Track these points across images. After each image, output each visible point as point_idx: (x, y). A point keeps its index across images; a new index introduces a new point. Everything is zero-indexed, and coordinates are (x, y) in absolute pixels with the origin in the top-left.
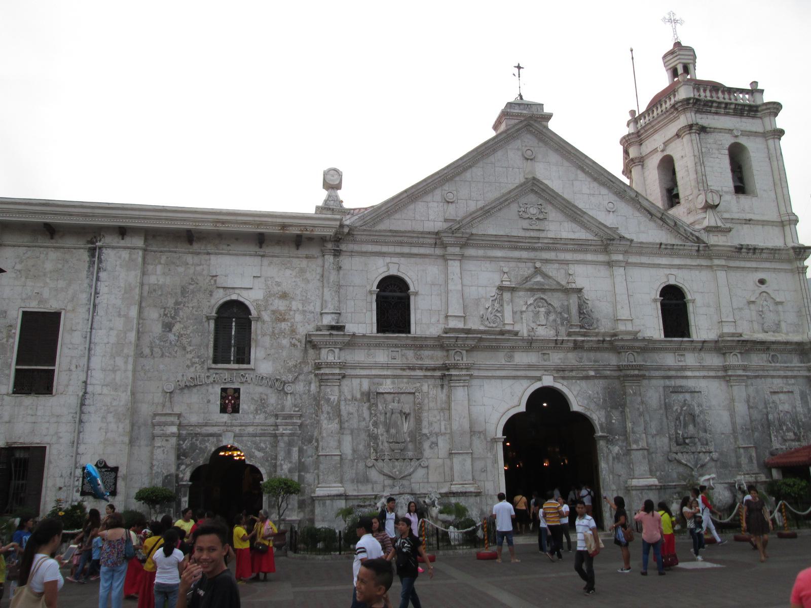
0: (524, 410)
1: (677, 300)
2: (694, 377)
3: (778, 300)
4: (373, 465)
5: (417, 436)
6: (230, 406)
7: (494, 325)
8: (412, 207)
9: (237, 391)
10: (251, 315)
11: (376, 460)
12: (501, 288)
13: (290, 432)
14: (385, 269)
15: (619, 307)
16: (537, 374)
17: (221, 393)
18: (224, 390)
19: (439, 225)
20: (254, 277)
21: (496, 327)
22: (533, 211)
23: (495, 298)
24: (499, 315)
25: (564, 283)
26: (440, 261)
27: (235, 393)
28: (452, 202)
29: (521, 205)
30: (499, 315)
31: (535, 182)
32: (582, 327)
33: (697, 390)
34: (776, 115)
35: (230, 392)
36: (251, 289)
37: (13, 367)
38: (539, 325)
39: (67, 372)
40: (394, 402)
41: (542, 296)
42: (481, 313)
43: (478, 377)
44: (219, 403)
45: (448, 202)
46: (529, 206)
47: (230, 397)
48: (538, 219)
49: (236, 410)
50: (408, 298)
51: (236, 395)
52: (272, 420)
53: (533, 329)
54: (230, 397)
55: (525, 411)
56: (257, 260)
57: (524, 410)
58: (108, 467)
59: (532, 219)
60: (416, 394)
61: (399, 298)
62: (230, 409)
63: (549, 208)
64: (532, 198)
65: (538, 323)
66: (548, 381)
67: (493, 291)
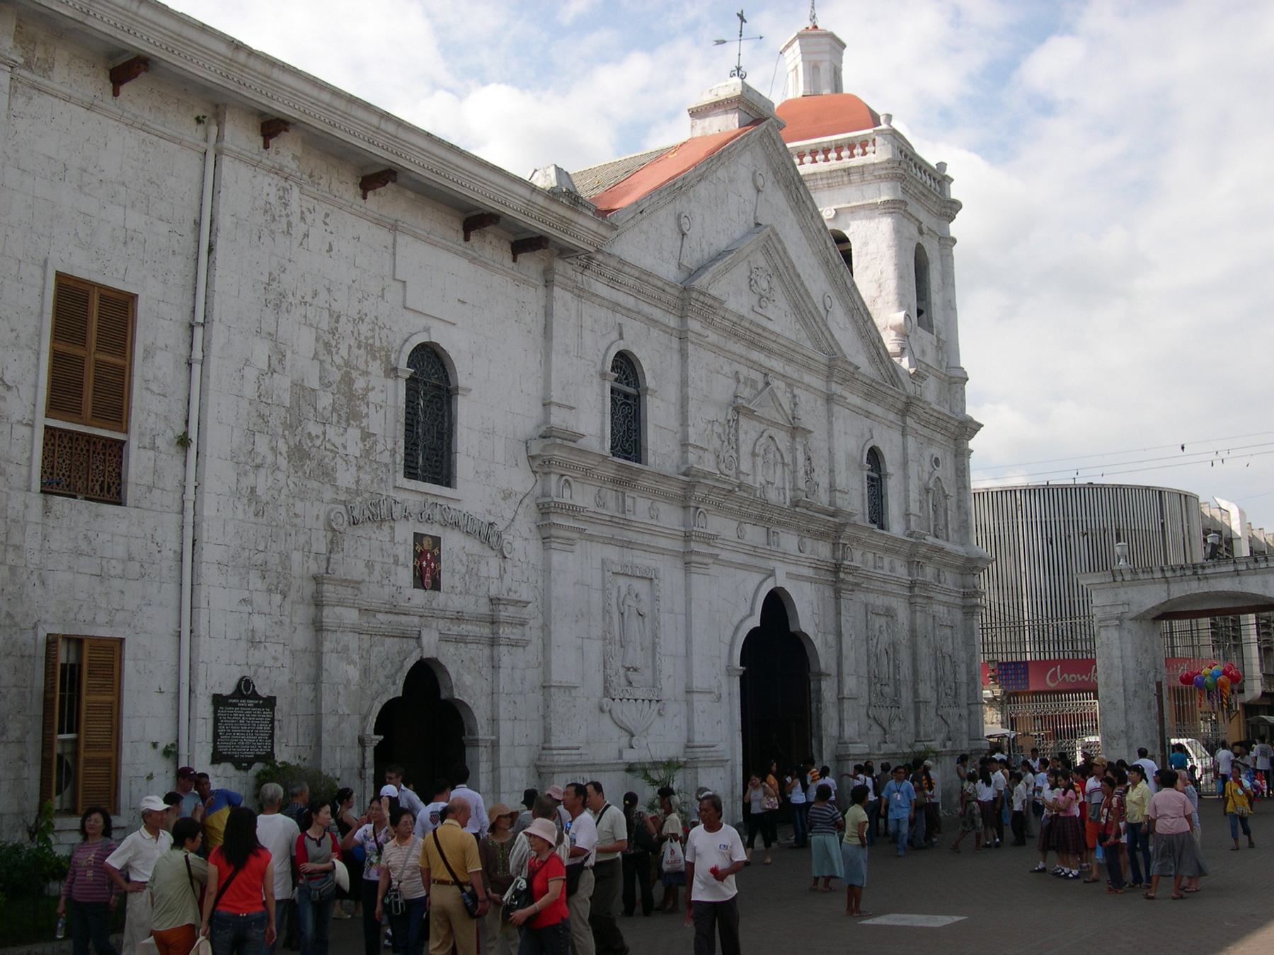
6: (428, 575)
9: (437, 541)
17: (415, 545)
18: (418, 537)
20: (459, 300)
27: (434, 548)
34: (952, 218)
35: (427, 543)
37: (42, 421)
38: (768, 483)
39: (151, 453)
44: (411, 565)
45: (684, 234)
47: (429, 555)
49: (436, 586)
50: (637, 398)
51: (436, 551)
52: (484, 609)
54: (429, 555)
58: (259, 698)
60: (656, 581)
61: (627, 396)
62: (428, 581)
66: (781, 581)
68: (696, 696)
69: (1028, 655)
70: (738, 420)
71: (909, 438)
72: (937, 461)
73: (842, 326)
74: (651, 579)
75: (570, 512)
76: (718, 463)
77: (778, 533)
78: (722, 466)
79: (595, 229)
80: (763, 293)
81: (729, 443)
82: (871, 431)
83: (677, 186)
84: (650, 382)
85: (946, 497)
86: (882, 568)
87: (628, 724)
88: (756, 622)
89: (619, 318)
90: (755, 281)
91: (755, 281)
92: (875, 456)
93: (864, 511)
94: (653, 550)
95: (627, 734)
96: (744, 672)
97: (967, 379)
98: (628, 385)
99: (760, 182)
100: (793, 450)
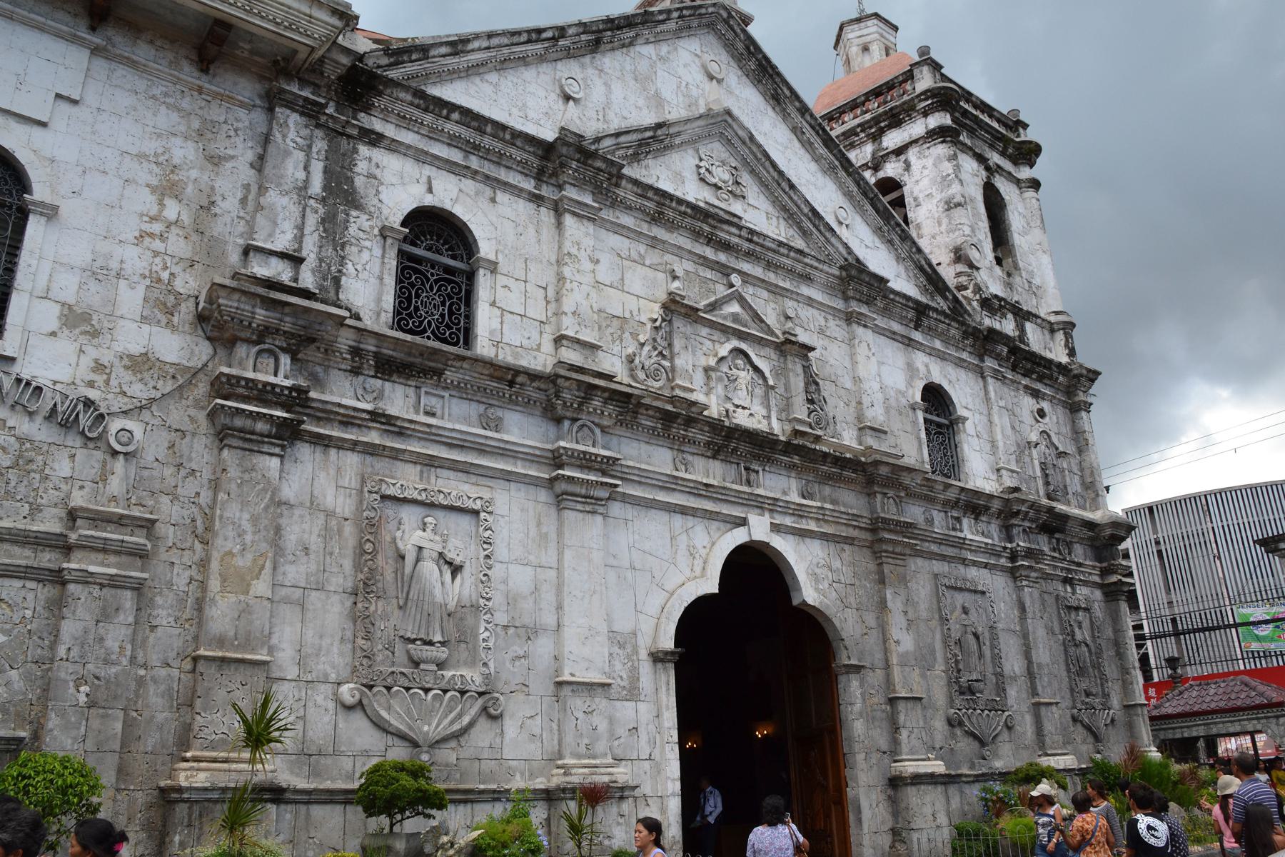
0: (712, 586)
1: (938, 415)
3: (1061, 449)
4: (360, 703)
5: (482, 630)
7: (657, 385)
8: (493, 77)
10: (30, 193)
11: (370, 687)
12: (674, 307)
13: (113, 571)
14: (422, 188)
15: (866, 401)
16: (737, 512)
19: (549, 135)
21: (660, 388)
22: (721, 175)
23: (658, 324)
24: (666, 364)
25: (779, 333)
26: (546, 215)
28: (574, 99)
29: (703, 156)
30: (666, 364)
31: (730, 120)
32: (811, 427)
33: (980, 588)
36: (43, 124)
38: (738, 406)
40: (424, 530)
41: (744, 346)
42: (630, 351)
43: (626, 499)
45: (567, 98)
46: (717, 163)
48: (730, 192)
50: (471, 276)
53: (727, 411)
55: (717, 591)
56: (77, 57)
57: (712, 586)
59: (720, 188)
60: (482, 515)
61: (448, 270)
63: (746, 178)
64: (716, 149)
65: (737, 402)
66: (759, 528)
67: (656, 311)
68: (566, 691)
69: (1241, 662)
70: (670, 321)
71: (990, 380)
72: (1041, 413)
73: (870, 245)
74: (476, 513)
75: (270, 397)
76: (632, 370)
77: (757, 472)
78: (641, 375)
79: (307, 11)
80: (720, 184)
81: (655, 349)
82: (927, 366)
83: (544, 35)
84: (486, 249)
85: (1061, 455)
86: (961, 531)
87: (402, 727)
88: (711, 585)
89: (428, 171)
90: (707, 170)
91: (707, 170)
92: (935, 397)
93: (923, 458)
94: (480, 471)
95: (407, 744)
96: (681, 655)
97: (1073, 325)
98: (454, 257)
99: (714, 68)
100: (781, 372)
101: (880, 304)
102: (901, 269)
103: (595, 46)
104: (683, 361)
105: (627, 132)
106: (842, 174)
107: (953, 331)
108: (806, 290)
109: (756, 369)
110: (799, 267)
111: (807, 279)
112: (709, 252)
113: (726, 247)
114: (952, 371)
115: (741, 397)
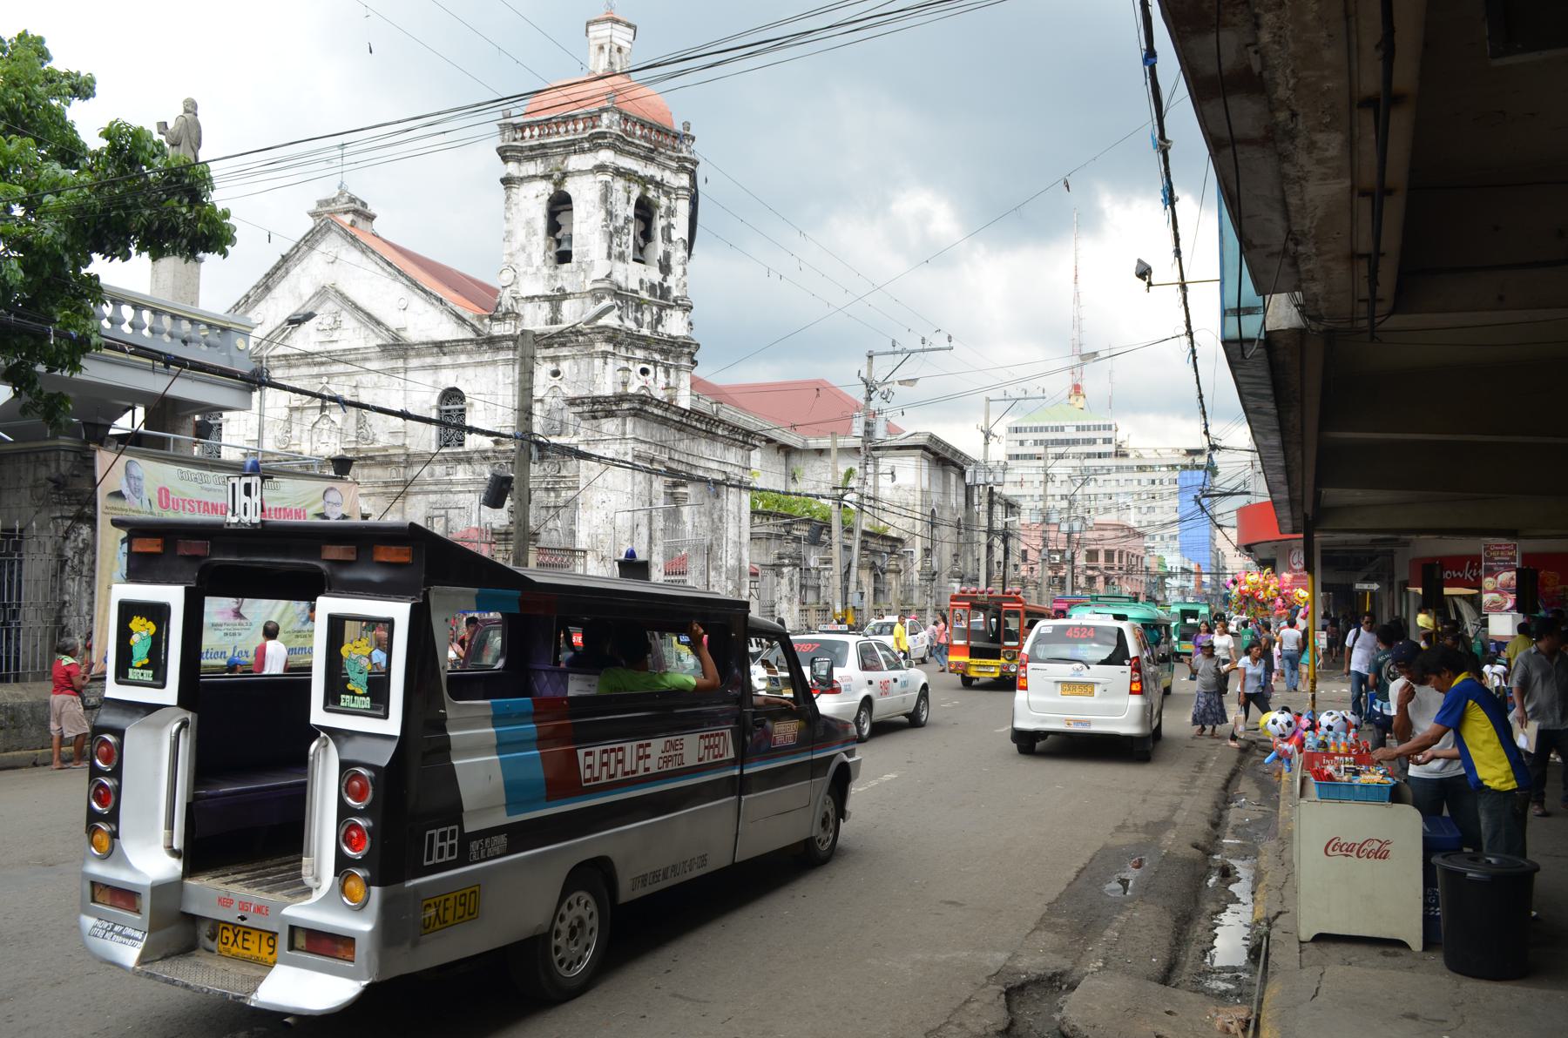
2: (460, 492)
32: (357, 442)
101: (412, 353)
102: (444, 317)
103: (268, 289)
104: (296, 431)
105: (272, 332)
106: (400, 278)
107: (469, 347)
108: (368, 365)
109: (333, 422)
110: (359, 356)
111: (366, 359)
112: (316, 370)
113: (322, 364)
114: (470, 372)
115: (325, 438)
